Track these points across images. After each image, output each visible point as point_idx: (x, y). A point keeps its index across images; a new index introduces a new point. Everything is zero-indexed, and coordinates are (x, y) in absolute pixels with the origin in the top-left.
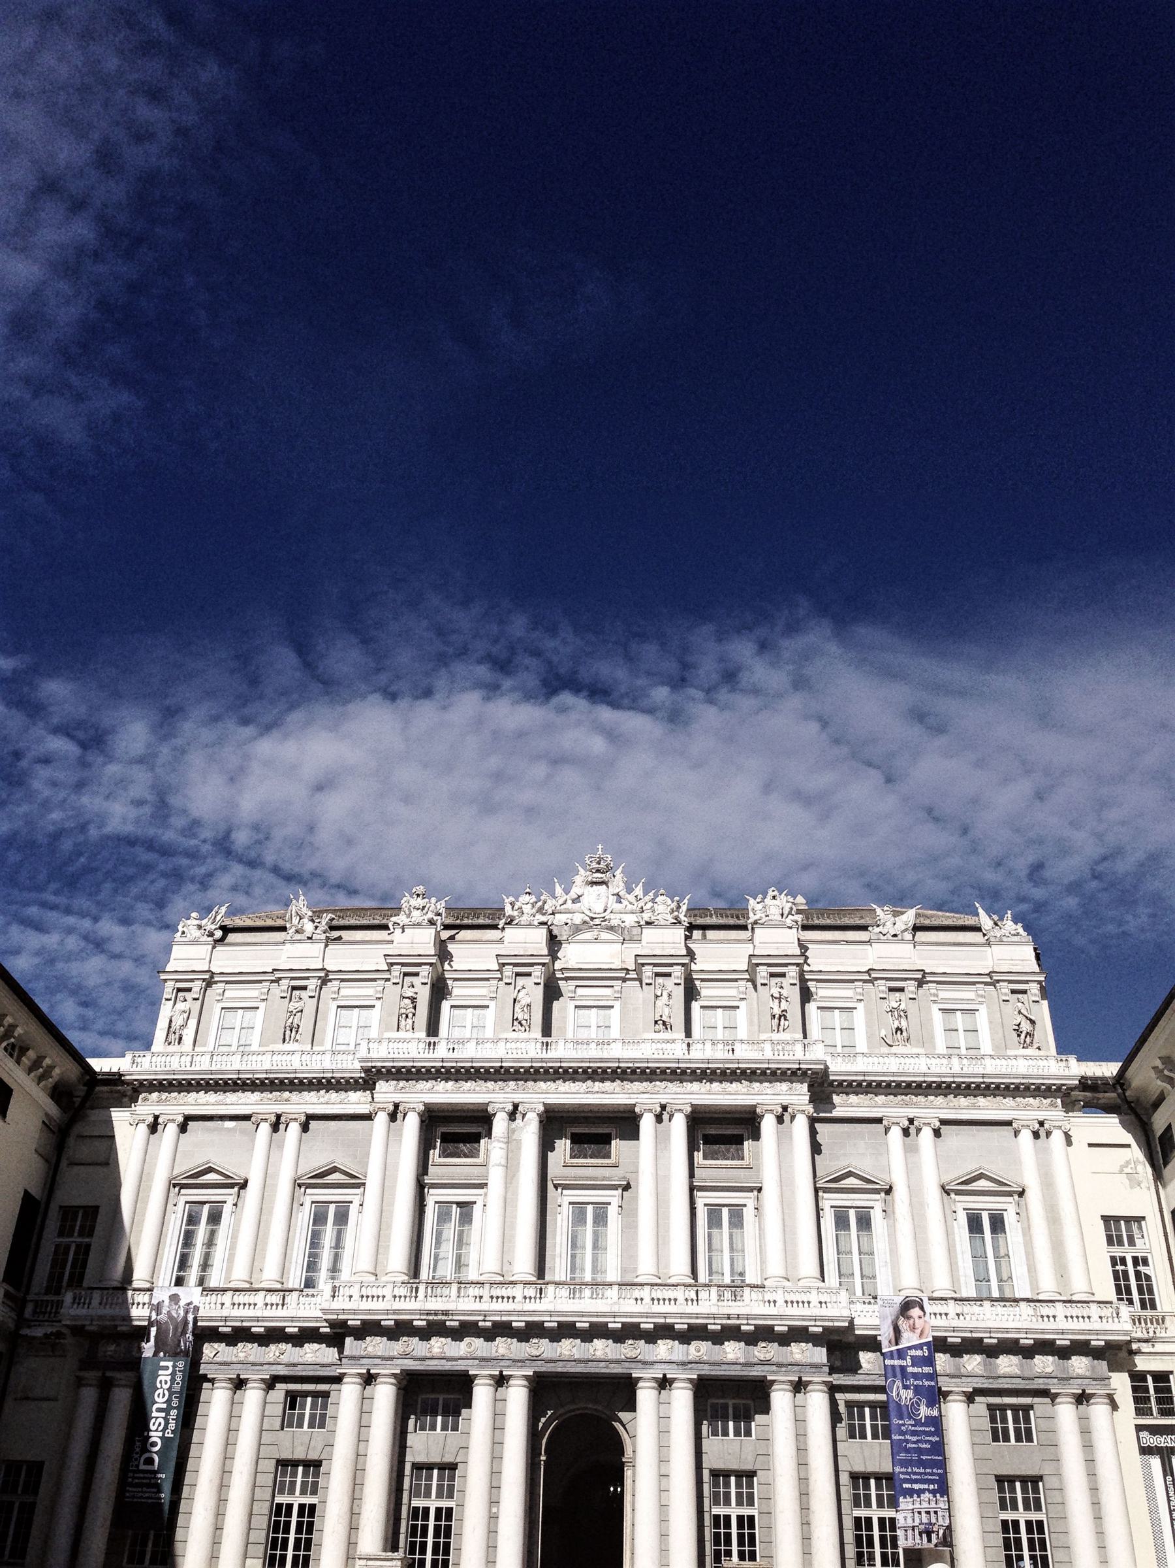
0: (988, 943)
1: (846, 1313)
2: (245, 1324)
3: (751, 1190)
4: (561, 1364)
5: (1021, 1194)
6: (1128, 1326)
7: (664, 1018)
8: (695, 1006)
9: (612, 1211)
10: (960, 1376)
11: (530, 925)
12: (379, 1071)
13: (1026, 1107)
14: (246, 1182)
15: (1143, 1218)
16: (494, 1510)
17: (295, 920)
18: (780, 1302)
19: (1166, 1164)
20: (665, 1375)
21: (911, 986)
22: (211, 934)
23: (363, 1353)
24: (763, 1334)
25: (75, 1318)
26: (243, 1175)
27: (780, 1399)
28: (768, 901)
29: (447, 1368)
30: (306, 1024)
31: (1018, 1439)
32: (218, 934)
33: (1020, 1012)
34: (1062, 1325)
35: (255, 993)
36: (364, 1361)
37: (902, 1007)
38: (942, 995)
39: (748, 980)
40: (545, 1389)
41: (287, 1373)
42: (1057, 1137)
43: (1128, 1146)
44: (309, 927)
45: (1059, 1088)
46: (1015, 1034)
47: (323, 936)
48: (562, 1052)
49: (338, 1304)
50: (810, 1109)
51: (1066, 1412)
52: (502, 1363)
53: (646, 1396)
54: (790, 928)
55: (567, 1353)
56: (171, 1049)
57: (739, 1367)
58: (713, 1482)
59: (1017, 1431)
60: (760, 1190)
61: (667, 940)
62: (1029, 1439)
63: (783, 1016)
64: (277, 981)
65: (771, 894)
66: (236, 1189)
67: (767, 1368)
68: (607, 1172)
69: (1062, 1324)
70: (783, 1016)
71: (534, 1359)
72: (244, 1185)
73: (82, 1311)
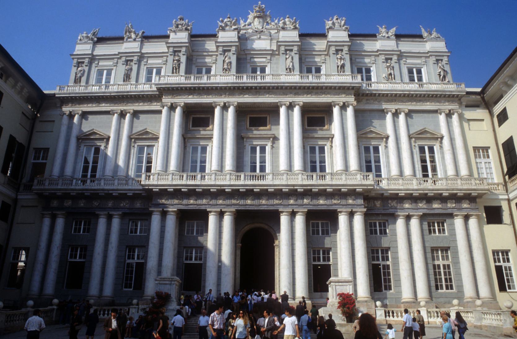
0: (426, 41)
3: (327, 138)
5: (442, 138)
7: (291, 67)
8: (303, 66)
9: (268, 149)
11: (230, 31)
12: (164, 88)
14: (109, 137)
15: (489, 147)
17: (128, 34)
19: (500, 126)
20: (293, 210)
21: (395, 58)
22: (92, 39)
24: (338, 193)
25: (37, 190)
26: (108, 134)
28: (334, 20)
32: (96, 39)
35: (111, 63)
36: (160, 206)
37: (392, 65)
38: (408, 61)
39: (326, 55)
40: (240, 217)
42: (456, 115)
43: (483, 120)
44: (133, 36)
45: (458, 95)
46: (438, 76)
47: (140, 39)
48: (246, 80)
49: (147, 183)
50: (355, 103)
51: (458, 222)
52: (222, 206)
53: (284, 220)
54: (345, 31)
57: (325, 206)
60: (332, 138)
61: (292, 36)
63: (343, 66)
64: (121, 57)
65: (335, 18)
68: (265, 132)
70: (343, 66)
72: (108, 139)
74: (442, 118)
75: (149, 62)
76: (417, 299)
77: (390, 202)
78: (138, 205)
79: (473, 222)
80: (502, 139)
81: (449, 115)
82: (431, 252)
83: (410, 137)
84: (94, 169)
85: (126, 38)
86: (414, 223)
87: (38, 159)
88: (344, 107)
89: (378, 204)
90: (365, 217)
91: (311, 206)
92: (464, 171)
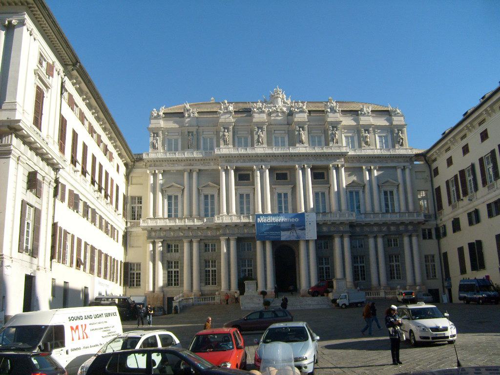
1: (355, 218)
5: (398, 186)
6: (423, 218)
10: (381, 232)
13: (401, 162)
14: (184, 189)
18: (338, 217)
19: (435, 176)
24: (333, 224)
27: (337, 241)
30: (195, 143)
31: (394, 245)
33: (400, 136)
34: (407, 218)
56: (156, 151)
58: (320, 259)
59: (394, 244)
62: (397, 245)
69: (407, 218)
72: (183, 190)
73: (146, 225)
74: (399, 171)
75: (204, 133)
76: (380, 285)
77: (365, 228)
78: (209, 233)
79: (414, 239)
80: (436, 186)
81: (404, 169)
82: (389, 258)
83: (379, 186)
84: (176, 211)
85: (186, 115)
86: (380, 241)
87: (135, 203)
88: (337, 169)
89: (358, 229)
90: (350, 239)
92: (411, 208)
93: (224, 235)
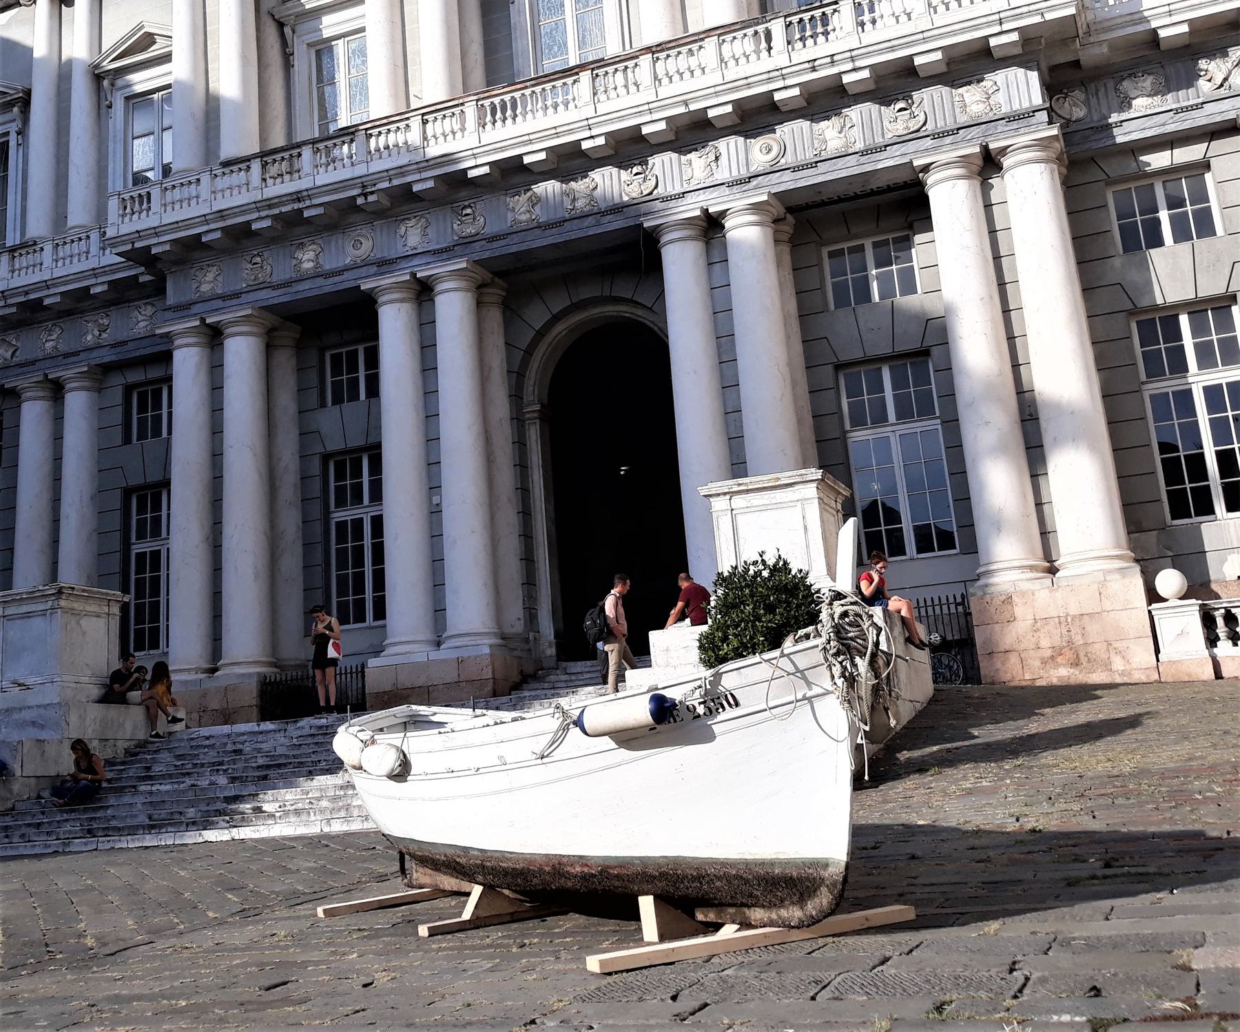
2: (32, 296)
4: (515, 238)
14: (28, 93)
16: (435, 500)
23: (194, 297)
29: (327, 290)
36: (196, 309)
41: (114, 358)
49: (128, 227)
52: (416, 262)
55: (524, 217)
57: (852, 160)
66: (15, 109)
67: (911, 146)
71: (465, 243)
72: (25, 101)
91: (788, 176)
93: (182, 309)
